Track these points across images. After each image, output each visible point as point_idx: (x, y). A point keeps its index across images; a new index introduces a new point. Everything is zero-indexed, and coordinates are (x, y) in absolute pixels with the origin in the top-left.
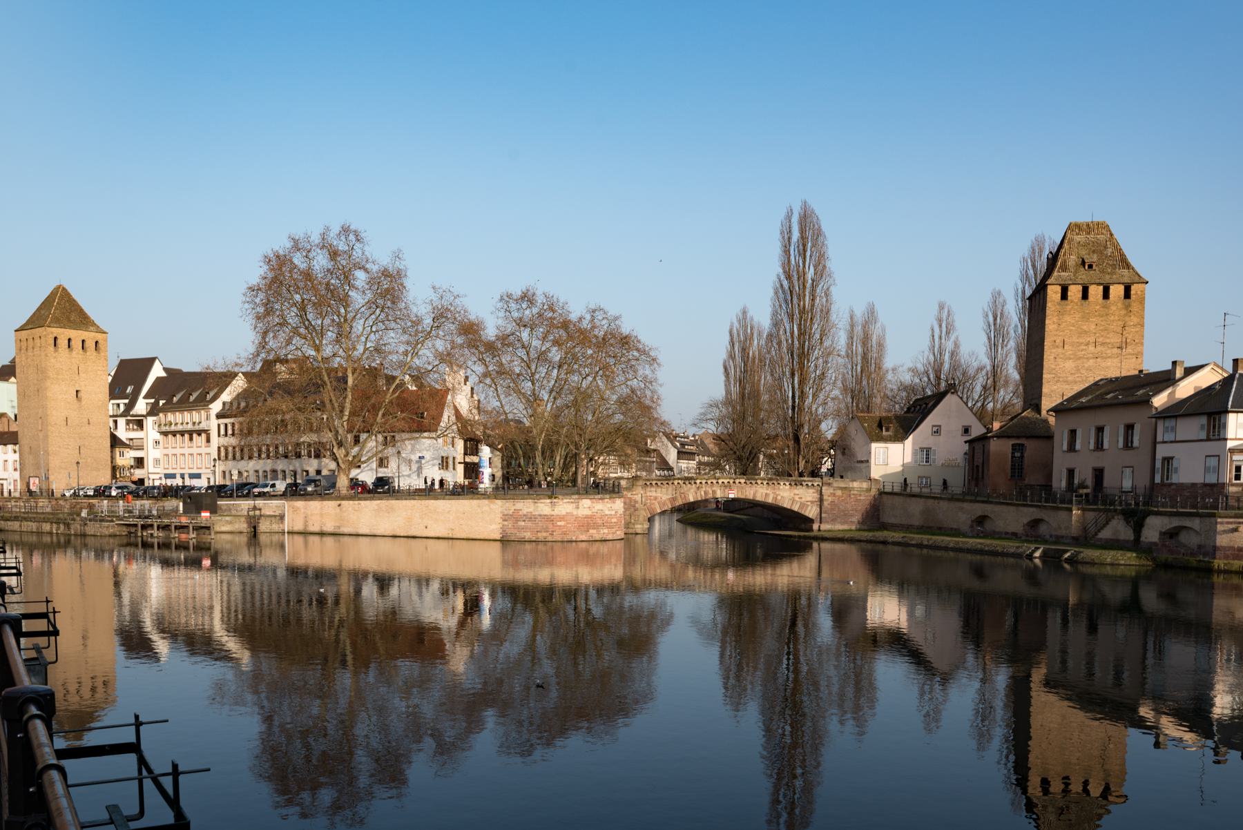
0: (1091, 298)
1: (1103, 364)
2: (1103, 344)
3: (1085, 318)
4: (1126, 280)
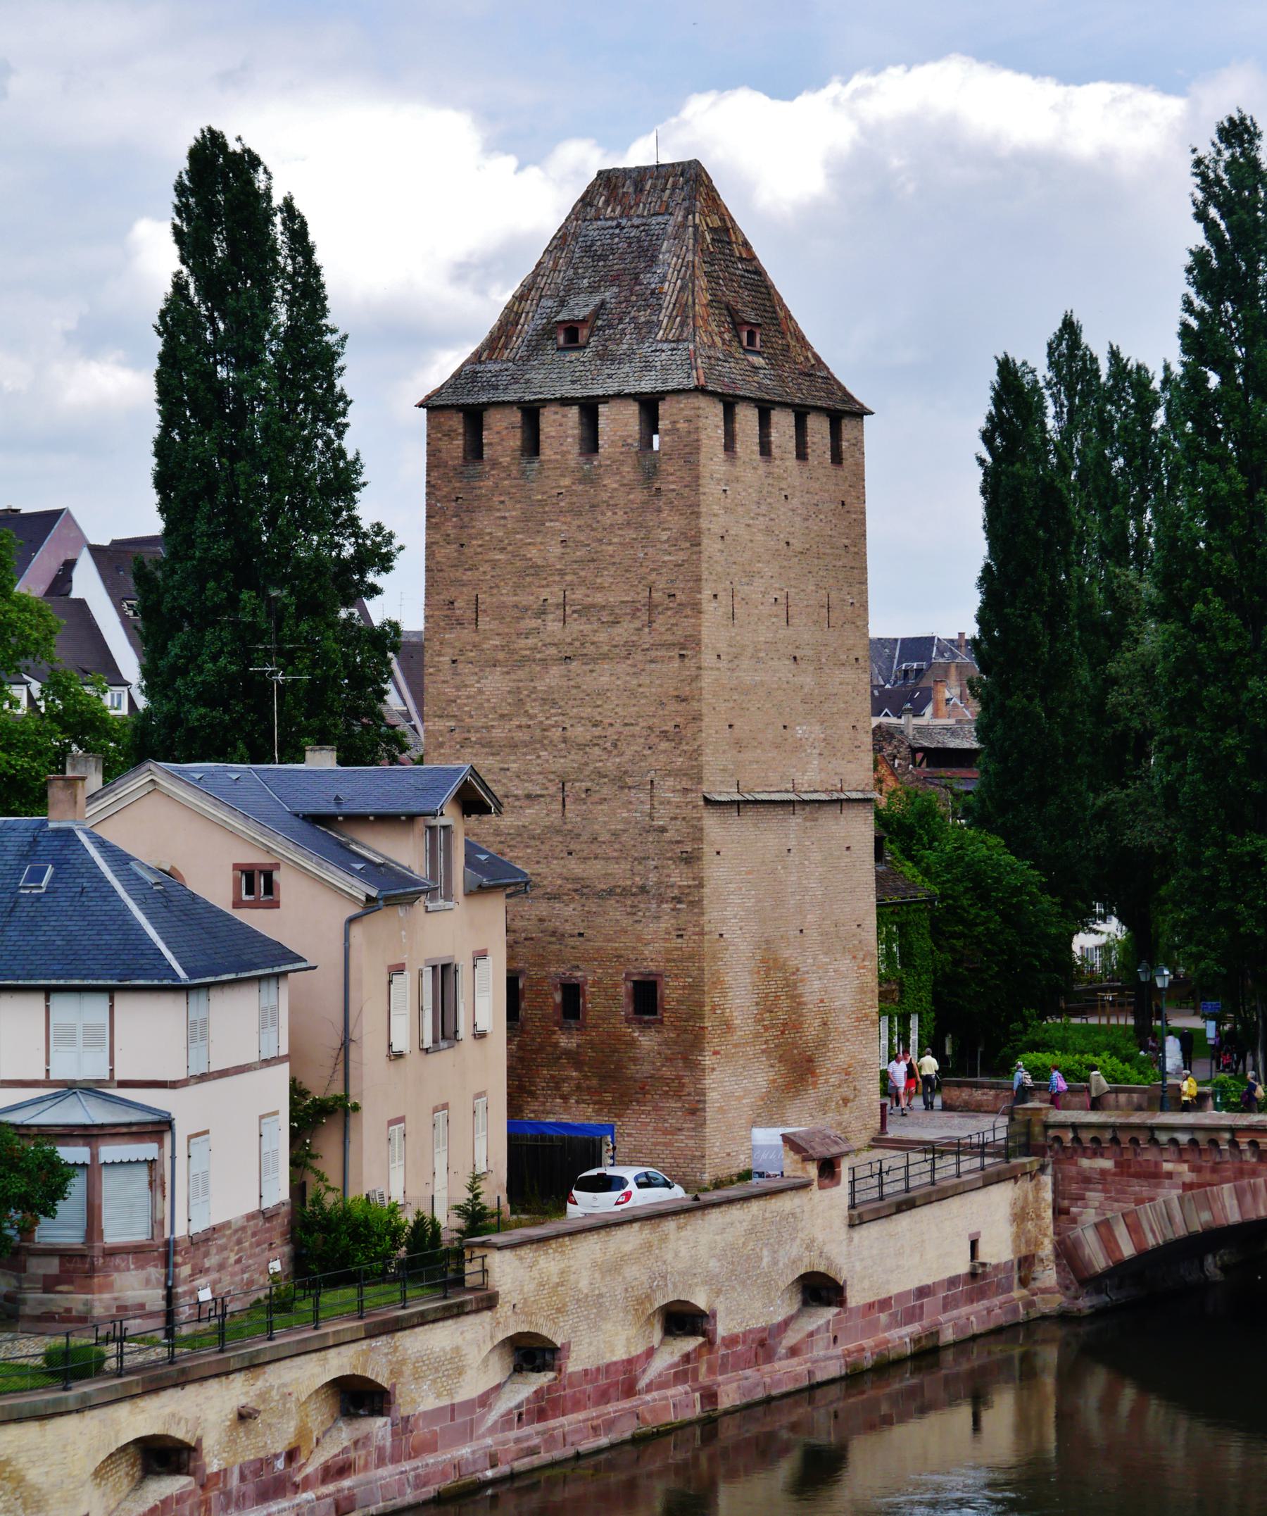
0: (547, 452)
1: (589, 683)
2: (585, 610)
3: (533, 521)
4: (646, 386)
